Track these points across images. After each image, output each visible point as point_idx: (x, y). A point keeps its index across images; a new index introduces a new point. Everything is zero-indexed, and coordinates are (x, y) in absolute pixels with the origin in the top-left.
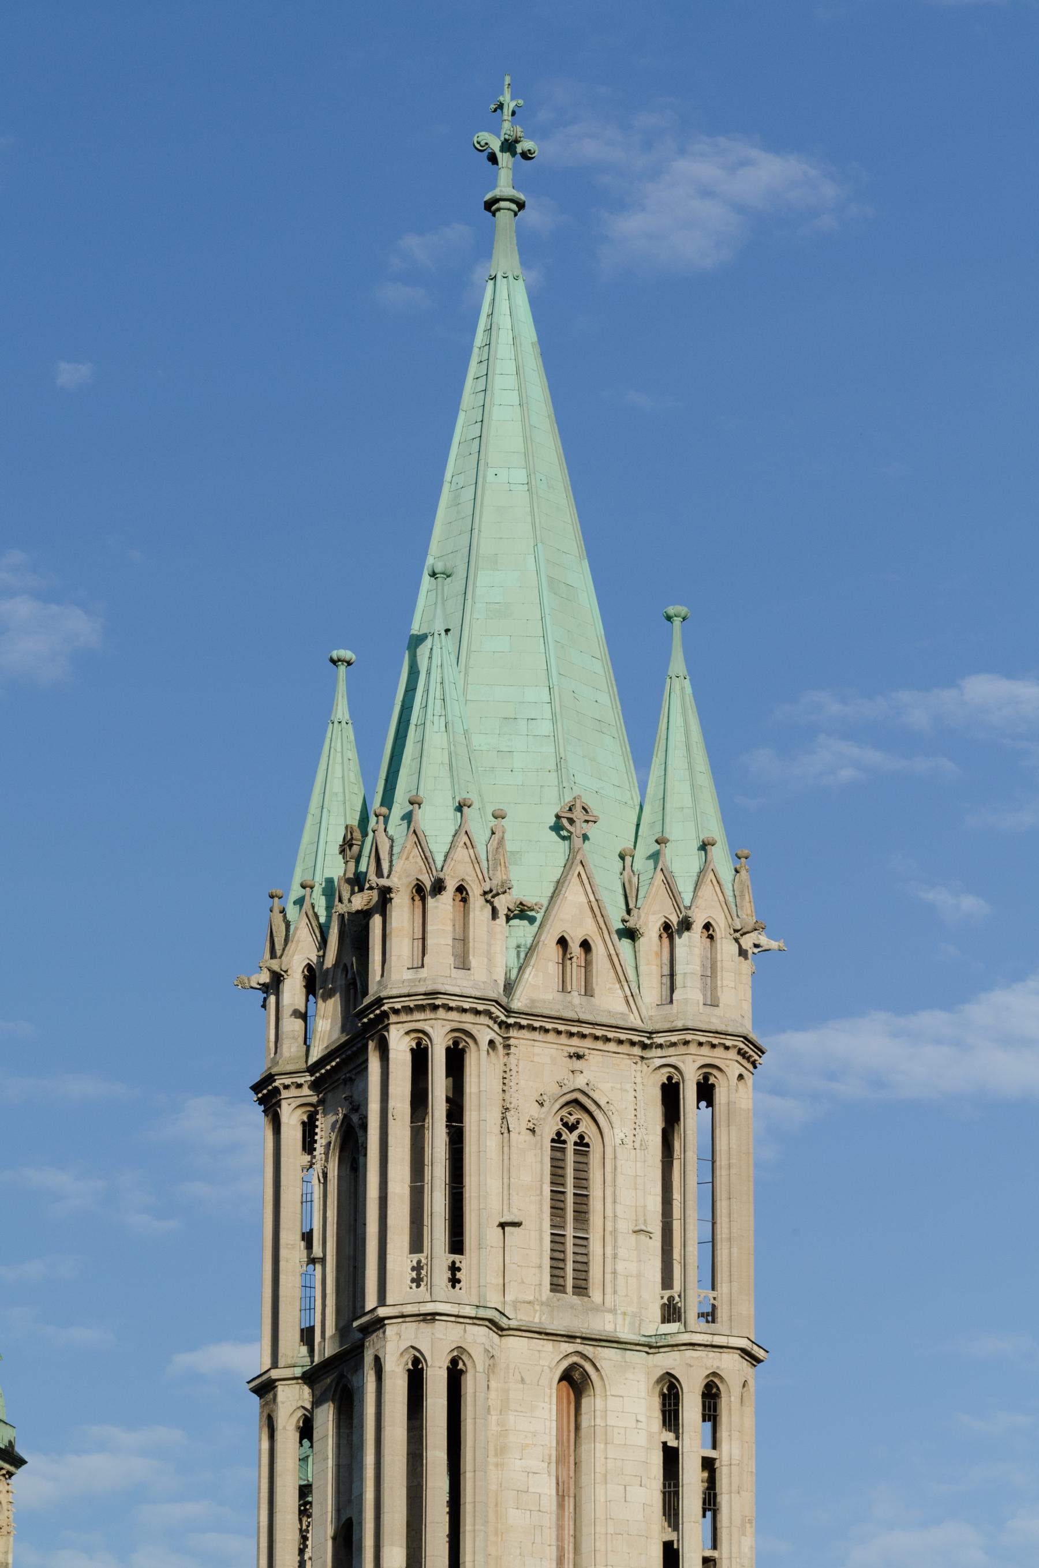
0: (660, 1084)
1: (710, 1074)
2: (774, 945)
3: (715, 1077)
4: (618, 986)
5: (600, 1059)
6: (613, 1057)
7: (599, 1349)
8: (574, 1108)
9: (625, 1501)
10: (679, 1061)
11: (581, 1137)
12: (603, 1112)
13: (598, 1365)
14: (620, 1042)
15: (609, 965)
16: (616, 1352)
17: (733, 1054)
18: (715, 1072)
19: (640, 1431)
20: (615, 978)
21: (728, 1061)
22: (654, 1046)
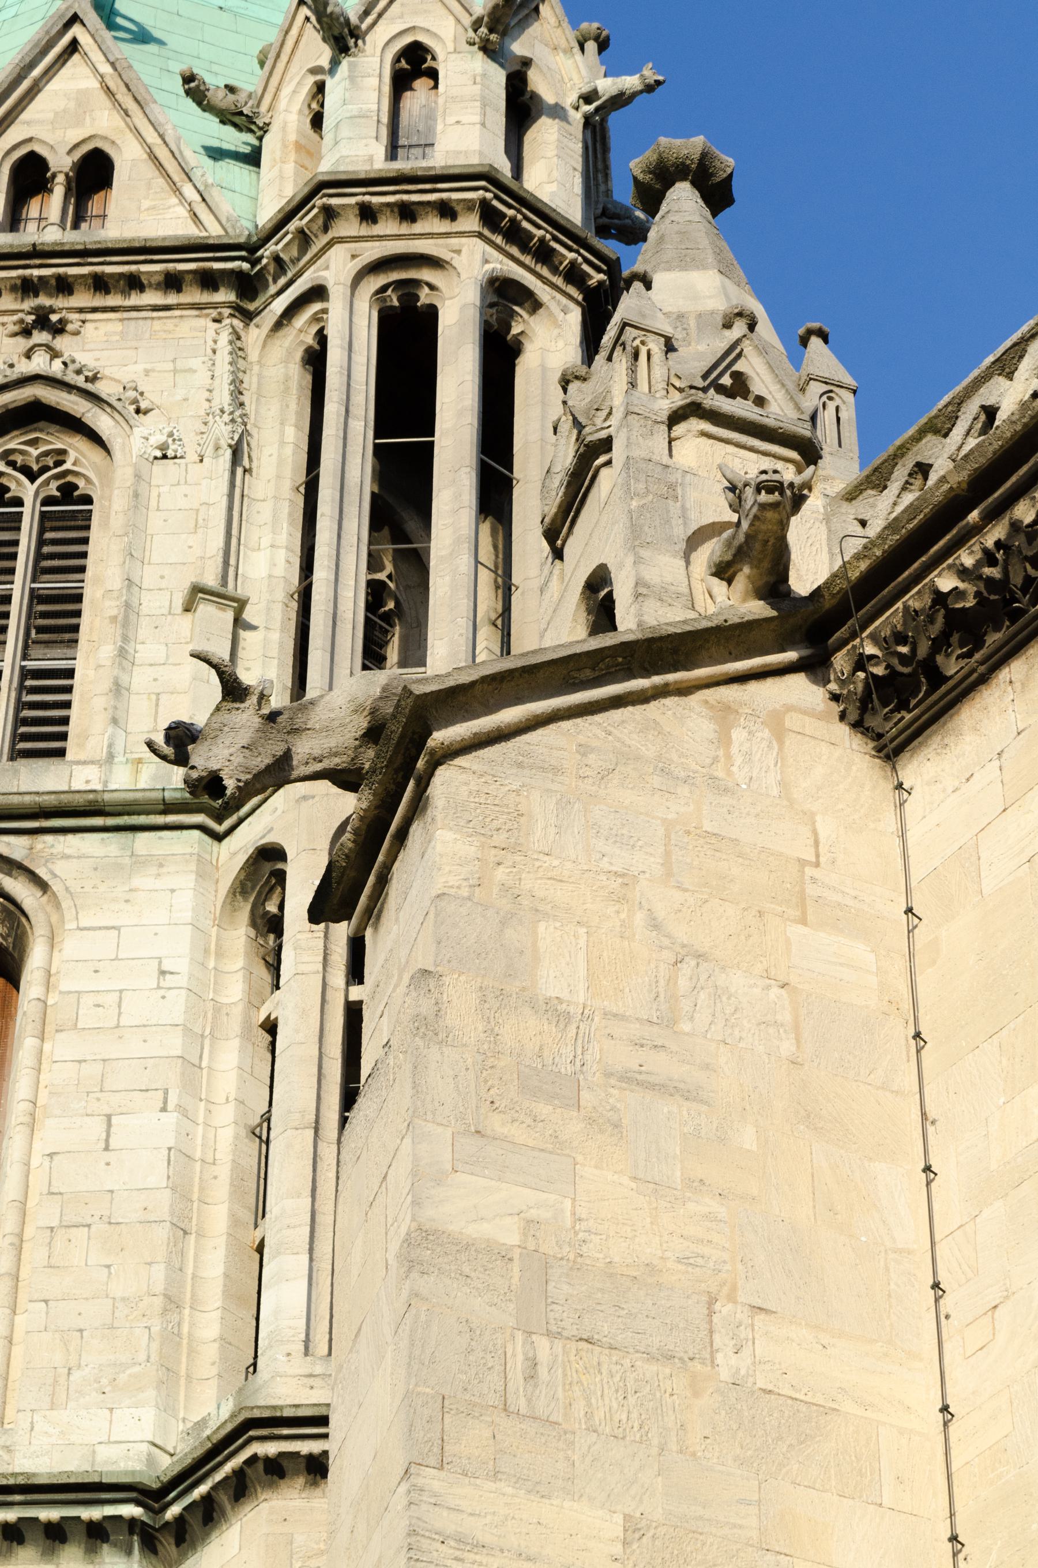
0: (299, 354)
1: (416, 283)
2: (631, 82)
3: (432, 287)
4: (174, 200)
5: (118, 327)
6: (153, 318)
7: (49, 838)
8: (41, 430)
9: (107, 1148)
10: (315, 272)
11: (68, 492)
12: (109, 410)
13: (42, 872)
14: (172, 282)
15: (149, 170)
16: (103, 839)
17: (471, 222)
18: (426, 275)
19: (170, 994)
20: (168, 188)
21: (454, 241)
22: (270, 279)
